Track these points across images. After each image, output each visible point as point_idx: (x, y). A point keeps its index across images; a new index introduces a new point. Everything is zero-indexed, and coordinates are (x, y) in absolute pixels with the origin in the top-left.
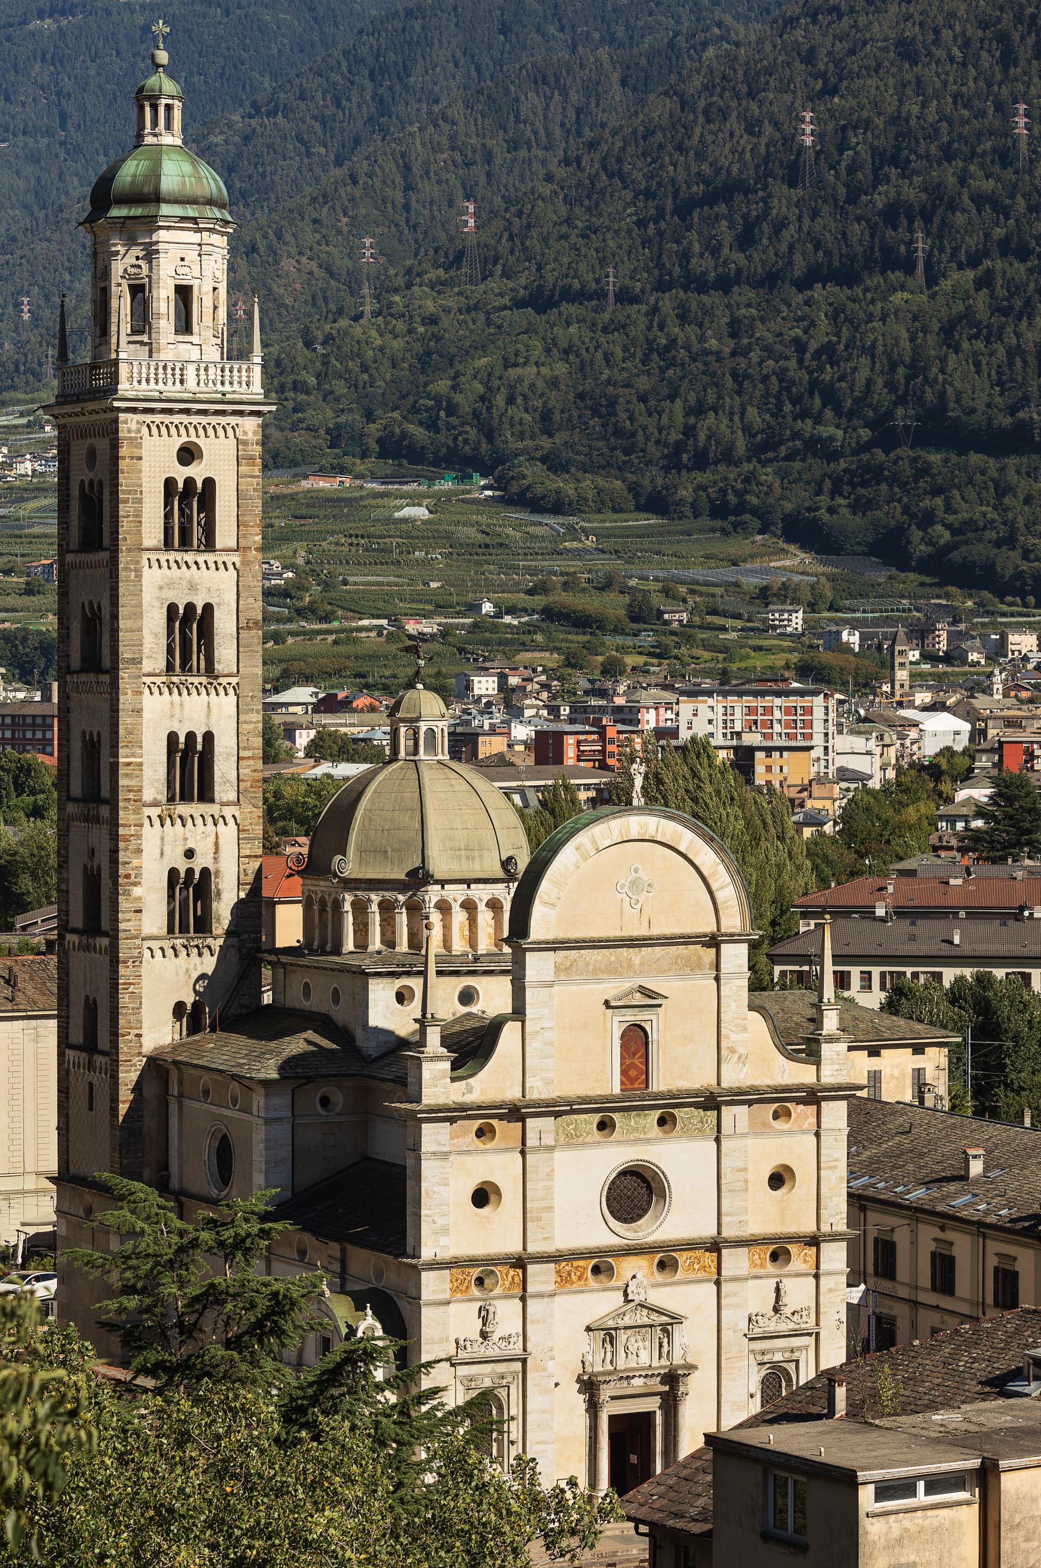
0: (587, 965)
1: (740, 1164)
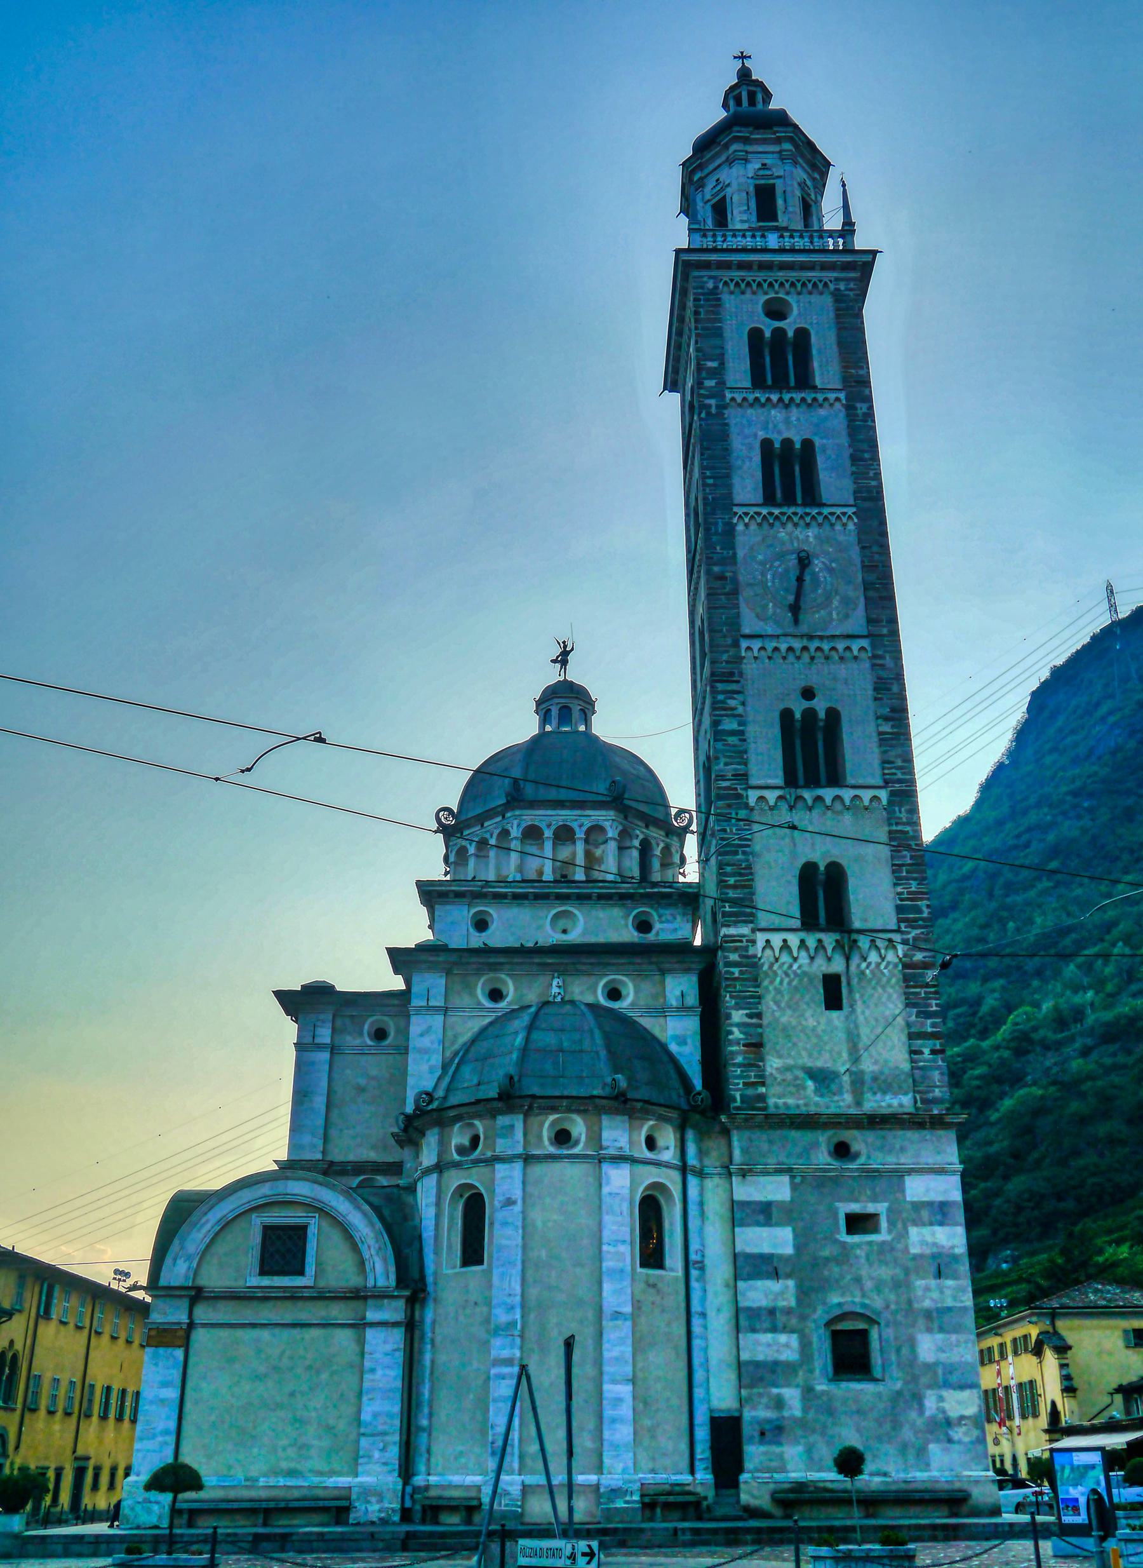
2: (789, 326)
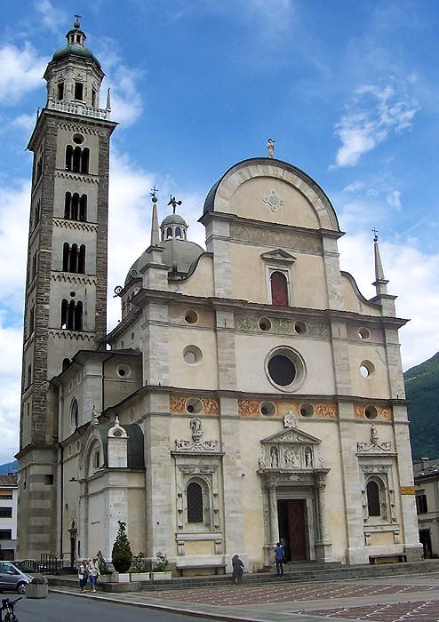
1: (343, 356)
2: (82, 146)
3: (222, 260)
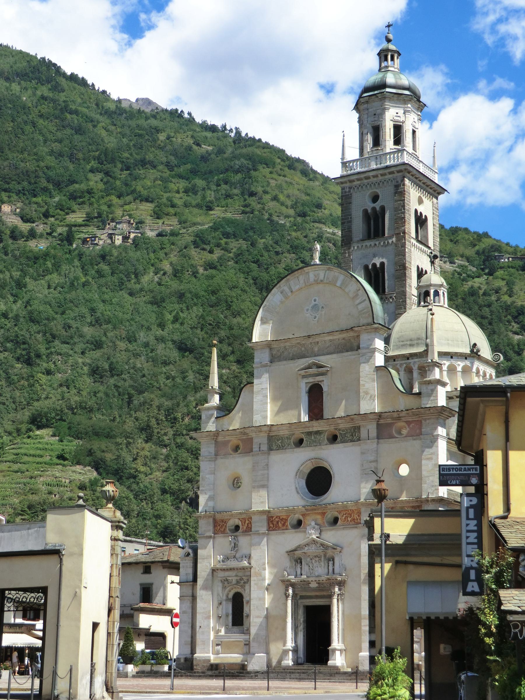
0: (289, 353)
1: (372, 458)
3: (261, 387)
